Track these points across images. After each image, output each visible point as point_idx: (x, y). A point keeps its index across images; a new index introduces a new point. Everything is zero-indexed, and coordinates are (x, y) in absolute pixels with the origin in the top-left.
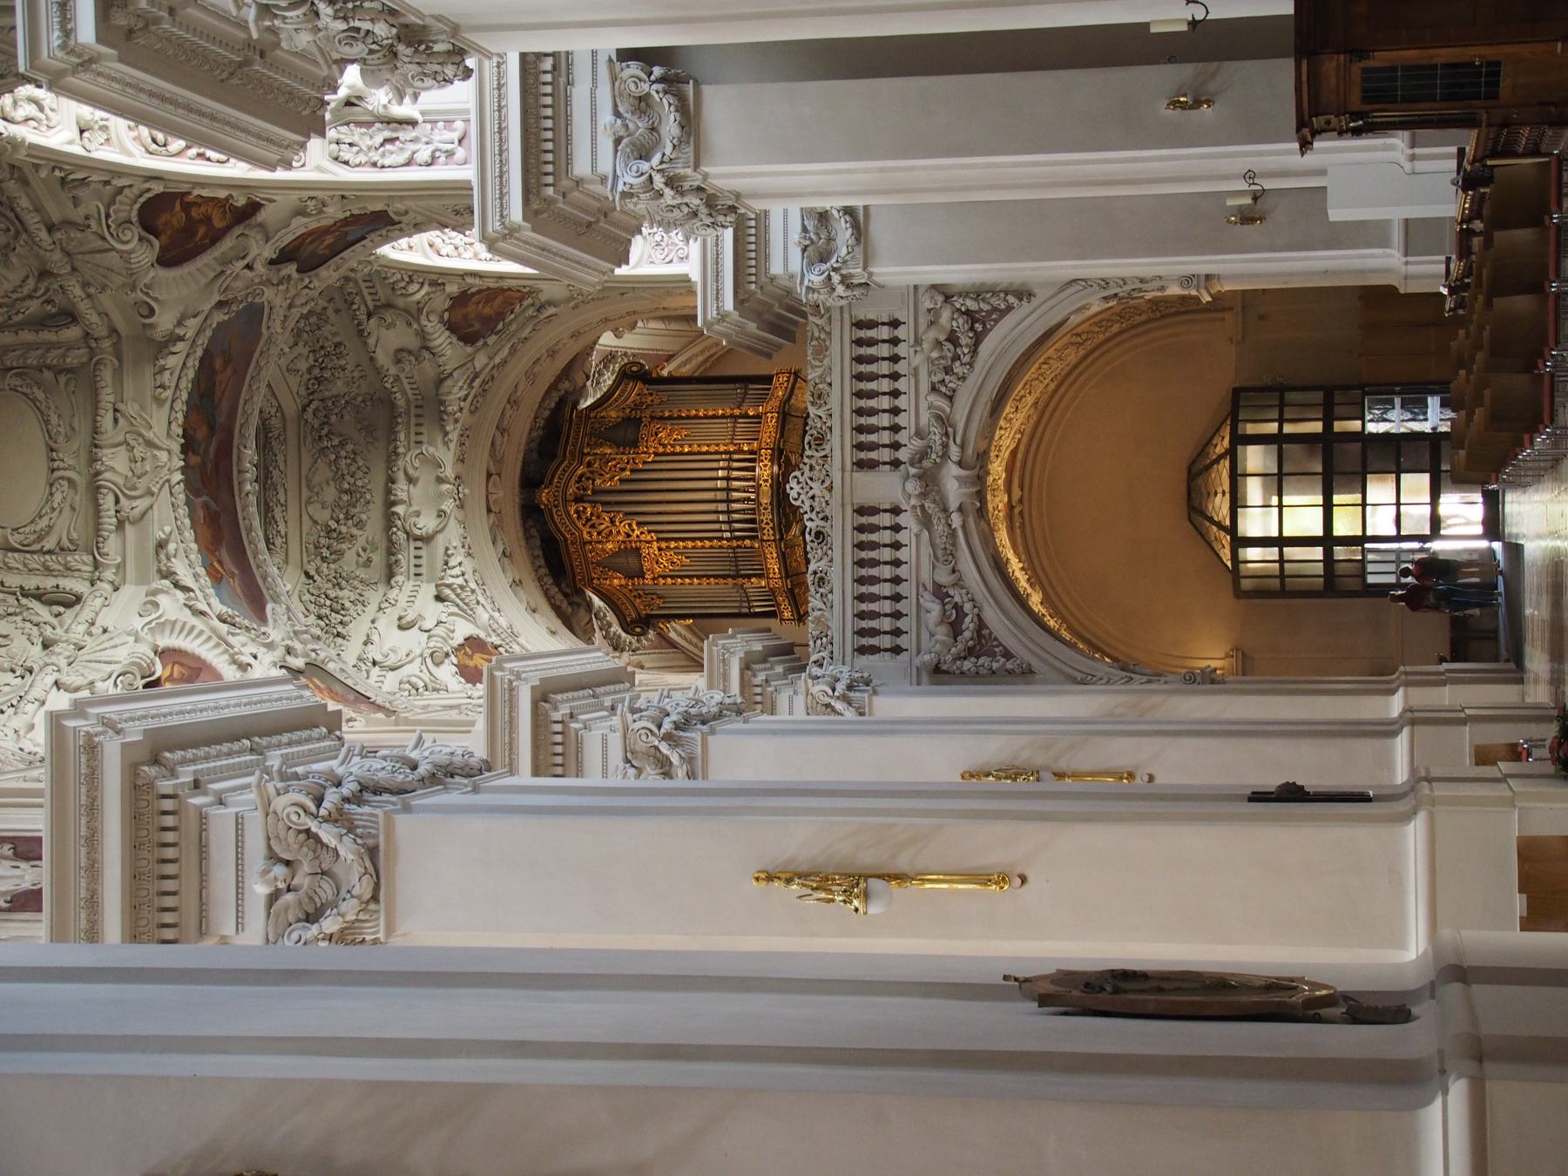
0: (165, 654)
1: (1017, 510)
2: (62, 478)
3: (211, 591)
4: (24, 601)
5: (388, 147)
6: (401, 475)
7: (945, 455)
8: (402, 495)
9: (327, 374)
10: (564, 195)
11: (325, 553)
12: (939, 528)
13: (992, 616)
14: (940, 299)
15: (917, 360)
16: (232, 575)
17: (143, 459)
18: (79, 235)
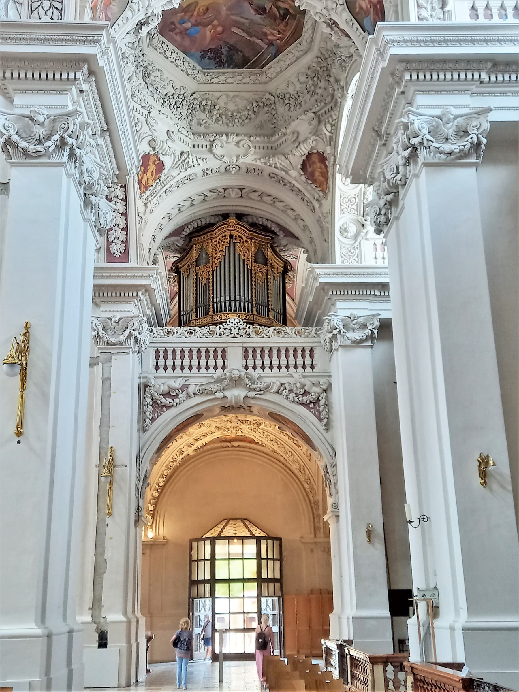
1: (228, 444)
6: (239, 138)
7: (250, 390)
8: (231, 138)
9: (287, 101)
11: (204, 103)
13: (172, 412)
14: (325, 387)
15: (296, 376)
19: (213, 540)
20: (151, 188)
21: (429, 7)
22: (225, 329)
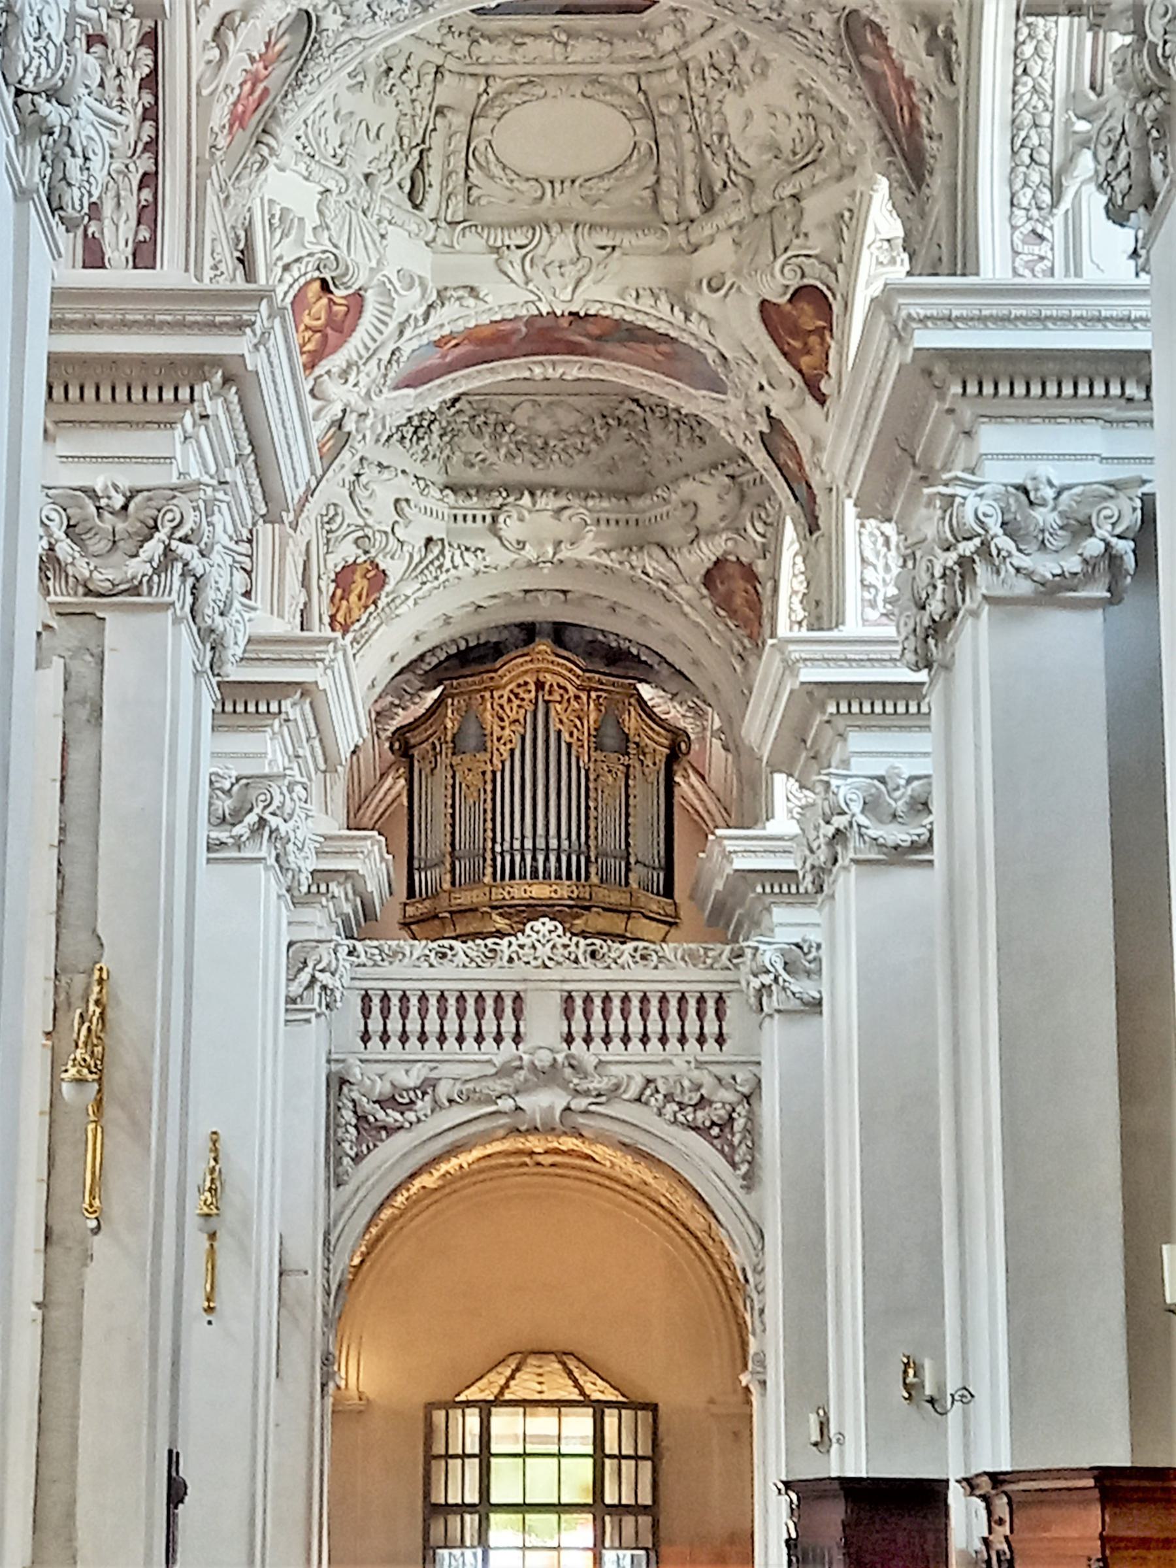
0: (357, 300)
1: (527, 1160)
2: (543, 194)
3: (425, 340)
4: (416, 152)
5: (881, 540)
8: (542, 502)
10: (828, 722)
11: (480, 420)
12: (498, 1086)
13: (401, 1141)
14: (745, 1090)
16: (444, 356)
17: (562, 275)
18: (789, 226)
19: (485, 1408)
20: (357, 626)
21: (880, 565)
22: (521, 947)
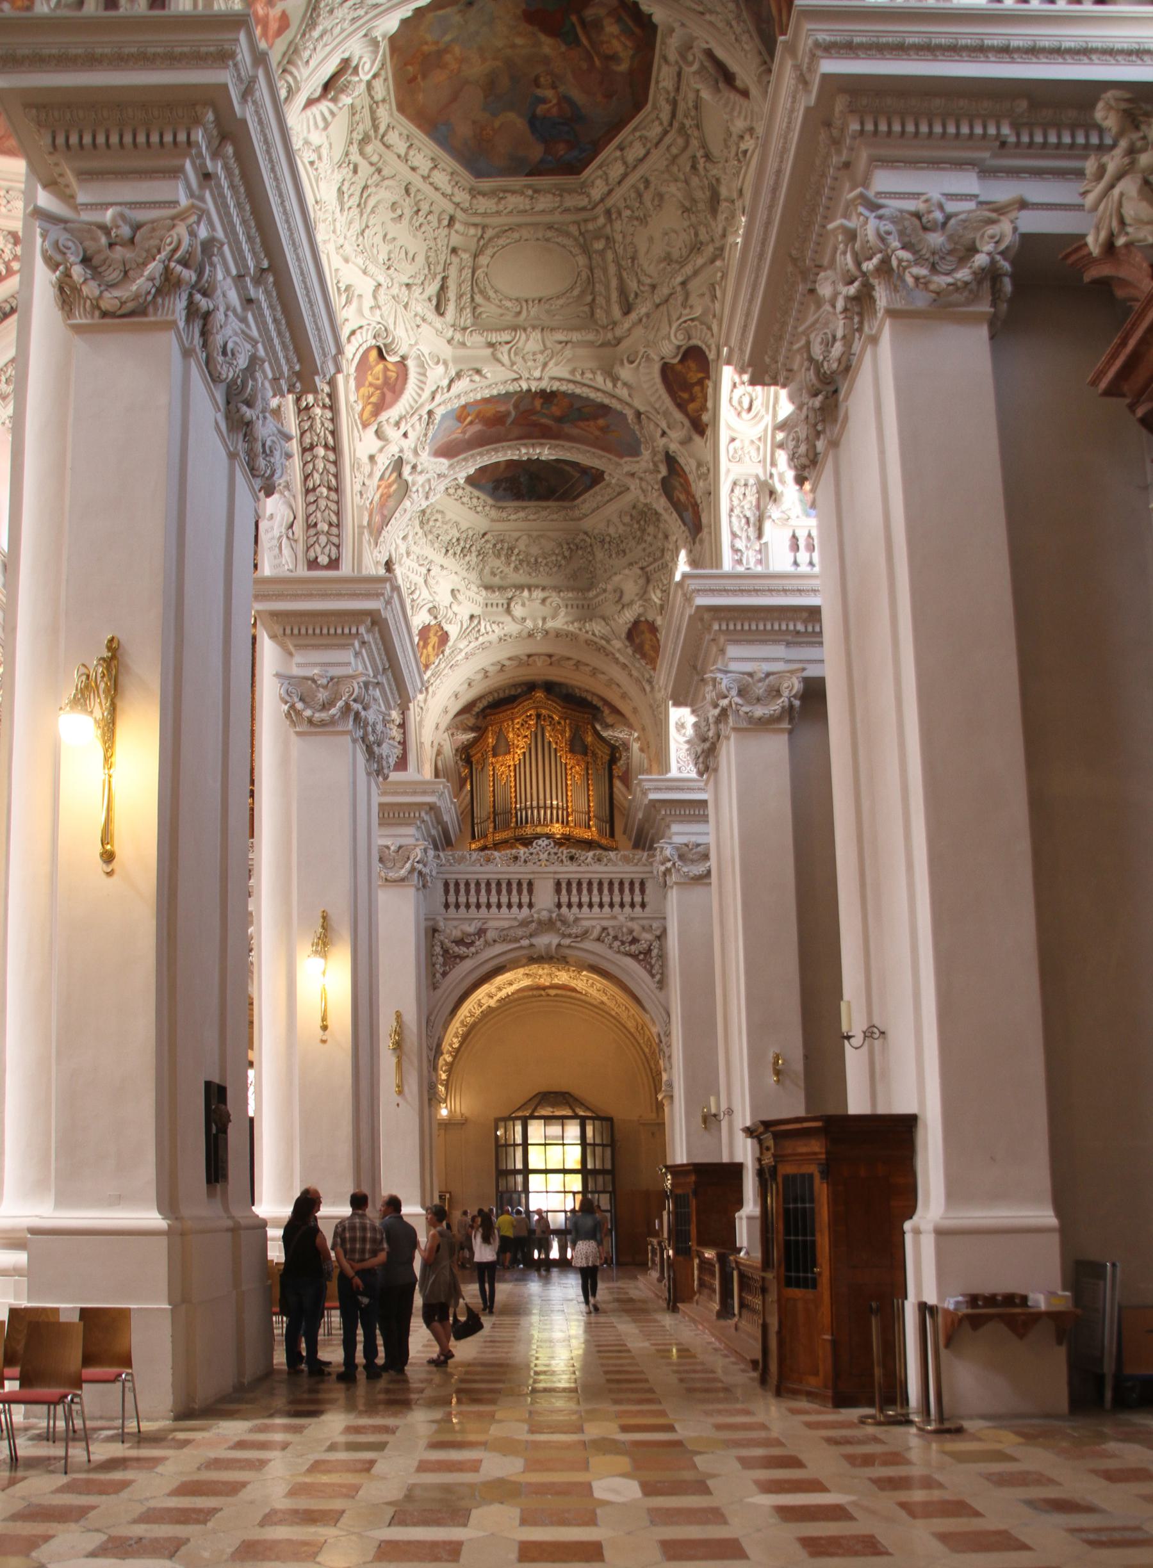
6: (546, 594)
7: (564, 936)
11: (499, 546)
12: (520, 932)
15: (621, 918)
22: (531, 854)
